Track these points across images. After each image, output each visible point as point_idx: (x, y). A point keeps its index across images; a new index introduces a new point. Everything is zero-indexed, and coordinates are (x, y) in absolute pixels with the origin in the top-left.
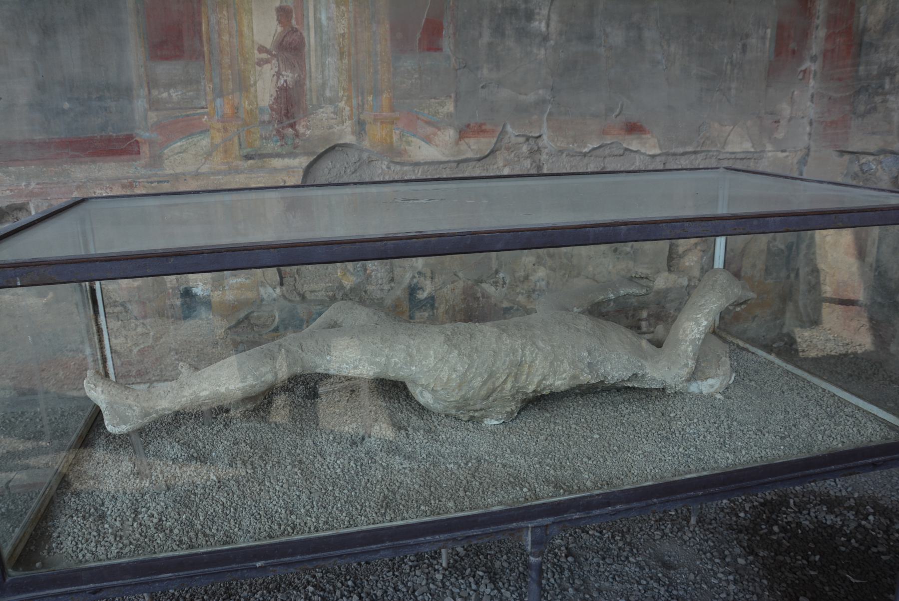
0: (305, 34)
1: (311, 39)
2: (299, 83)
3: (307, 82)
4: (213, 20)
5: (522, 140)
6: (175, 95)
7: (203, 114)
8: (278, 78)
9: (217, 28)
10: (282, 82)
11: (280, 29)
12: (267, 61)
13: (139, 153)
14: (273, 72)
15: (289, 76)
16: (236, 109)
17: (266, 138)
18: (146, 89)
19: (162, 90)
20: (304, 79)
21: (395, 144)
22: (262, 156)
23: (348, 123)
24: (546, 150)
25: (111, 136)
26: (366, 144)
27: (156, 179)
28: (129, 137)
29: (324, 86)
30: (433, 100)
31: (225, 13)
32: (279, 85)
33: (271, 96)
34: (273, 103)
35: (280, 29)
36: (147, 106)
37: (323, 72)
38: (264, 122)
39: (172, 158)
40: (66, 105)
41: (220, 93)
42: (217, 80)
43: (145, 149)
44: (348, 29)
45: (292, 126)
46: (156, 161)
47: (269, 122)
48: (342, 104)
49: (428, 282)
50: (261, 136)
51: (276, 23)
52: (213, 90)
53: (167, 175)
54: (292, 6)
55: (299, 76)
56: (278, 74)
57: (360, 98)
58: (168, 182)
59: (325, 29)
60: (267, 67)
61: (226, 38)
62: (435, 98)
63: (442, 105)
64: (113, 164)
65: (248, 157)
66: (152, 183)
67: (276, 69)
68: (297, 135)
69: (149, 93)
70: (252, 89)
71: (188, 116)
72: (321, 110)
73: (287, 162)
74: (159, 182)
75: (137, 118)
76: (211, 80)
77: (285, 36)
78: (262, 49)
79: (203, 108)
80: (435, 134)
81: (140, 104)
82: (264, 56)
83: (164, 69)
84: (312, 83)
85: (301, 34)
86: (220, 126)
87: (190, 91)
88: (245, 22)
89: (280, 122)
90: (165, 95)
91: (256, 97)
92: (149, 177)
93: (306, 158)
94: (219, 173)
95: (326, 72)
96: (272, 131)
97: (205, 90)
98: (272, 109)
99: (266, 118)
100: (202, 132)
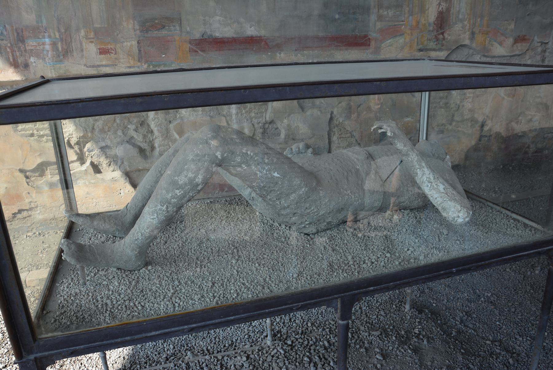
2: (448, 10)
3: (452, 9)
5: (539, 44)
6: (391, 13)
7: (402, 25)
8: (439, 7)
10: (441, 8)
13: (369, 45)
14: (437, 3)
16: (418, 22)
17: (430, 40)
18: (377, 9)
19: (384, 10)
20: (451, 8)
23: (468, 33)
24: (549, 50)
25: (357, 35)
26: (474, 45)
28: (366, 36)
29: (459, 12)
30: (506, 22)
32: (439, 10)
33: (435, 16)
34: (435, 21)
36: (376, 19)
38: (430, 31)
40: (337, 16)
41: (411, 13)
42: (411, 6)
43: (373, 43)
45: (443, 33)
47: (432, 31)
48: (466, 23)
49: (490, 121)
50: (428, 38)
52: (409, 11)
55: (449, 6)
56: (439, 4)
57: (474, 20)
62: (507, 21)
64: (356, 51)
65: (420, 50)
68: (444, 39)
69: (378, 11)
70: (427, 12)
71: (395, 25)
72: (457, 25)
75: (371, 25)
76: (408, 6)
79: (403, 21)
80: (504, 41)
81: (373, 17)
86: (409, 32)
87: (398, 11)
89: (437, 31)
90: (385, 13)
91: (428, 16)
93: (446, 51)
95: (461, 5)
96: (433, 36)
97: (405, 11)
98: (435, 24)
100: (401, 35)
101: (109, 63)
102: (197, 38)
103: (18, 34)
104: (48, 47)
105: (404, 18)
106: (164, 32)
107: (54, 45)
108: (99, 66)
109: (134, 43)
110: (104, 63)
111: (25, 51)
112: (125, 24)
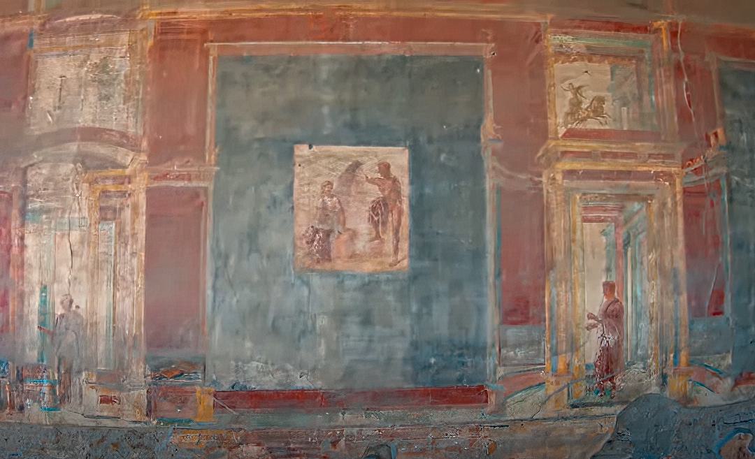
0: (624, 304)
1: (629, 308)
2: (618, 344)
3: (625, 343)
4: (554, 291)
6: (520, 353)
7: (541, 369)
9: (556, 299)
11: (605, 300)
12: (594, 326)
15: (611, 338)
20: (622, 340)
21: (688, 393)
22: (585, 405)
27: (498, 424)
28: (482, 387)
31: (563, 286)
32: (603, 345)
35: (605, 300)
37: (637, 333)
39: (512, 406)
44: (657, 299)
46: (501, 408)
47: (594, 376)
48: (649, 361)
51: (603, 295)
52: (551, 349)
53: (507, 421)
54: (615, 281)
55: (618, 338)
57: (664, 356)
58: (508, 426)
59: (639, 299)
60: (595, 329)
61: (563, 306)
63: (723, 358)
65: (574, 406)
66: (495, 427)
67: (602, 333)
70: (582, 349)
73: (605, 410)
74: (500, 426)
77: (609, 306)
78: (591, 316)
81: (491, 361)
82: (592, 321)
83: (512, 333)
84: (628, 345)
85: (621, 303)
86: (553, 379)
88: (579, 295)
92: (493, 422)
94: (549, 419)
99: (591, 373)
101: (111, 414)
102: (224, 389)
103: (18, 372)
104: (46, 389)
105: (543, 360)
106: (182, 381)
107: (52, 387)
108: (99, 417)
109: (144, 392)
110: (105, 414)
111: (23, 391)
112: (134, 368)
